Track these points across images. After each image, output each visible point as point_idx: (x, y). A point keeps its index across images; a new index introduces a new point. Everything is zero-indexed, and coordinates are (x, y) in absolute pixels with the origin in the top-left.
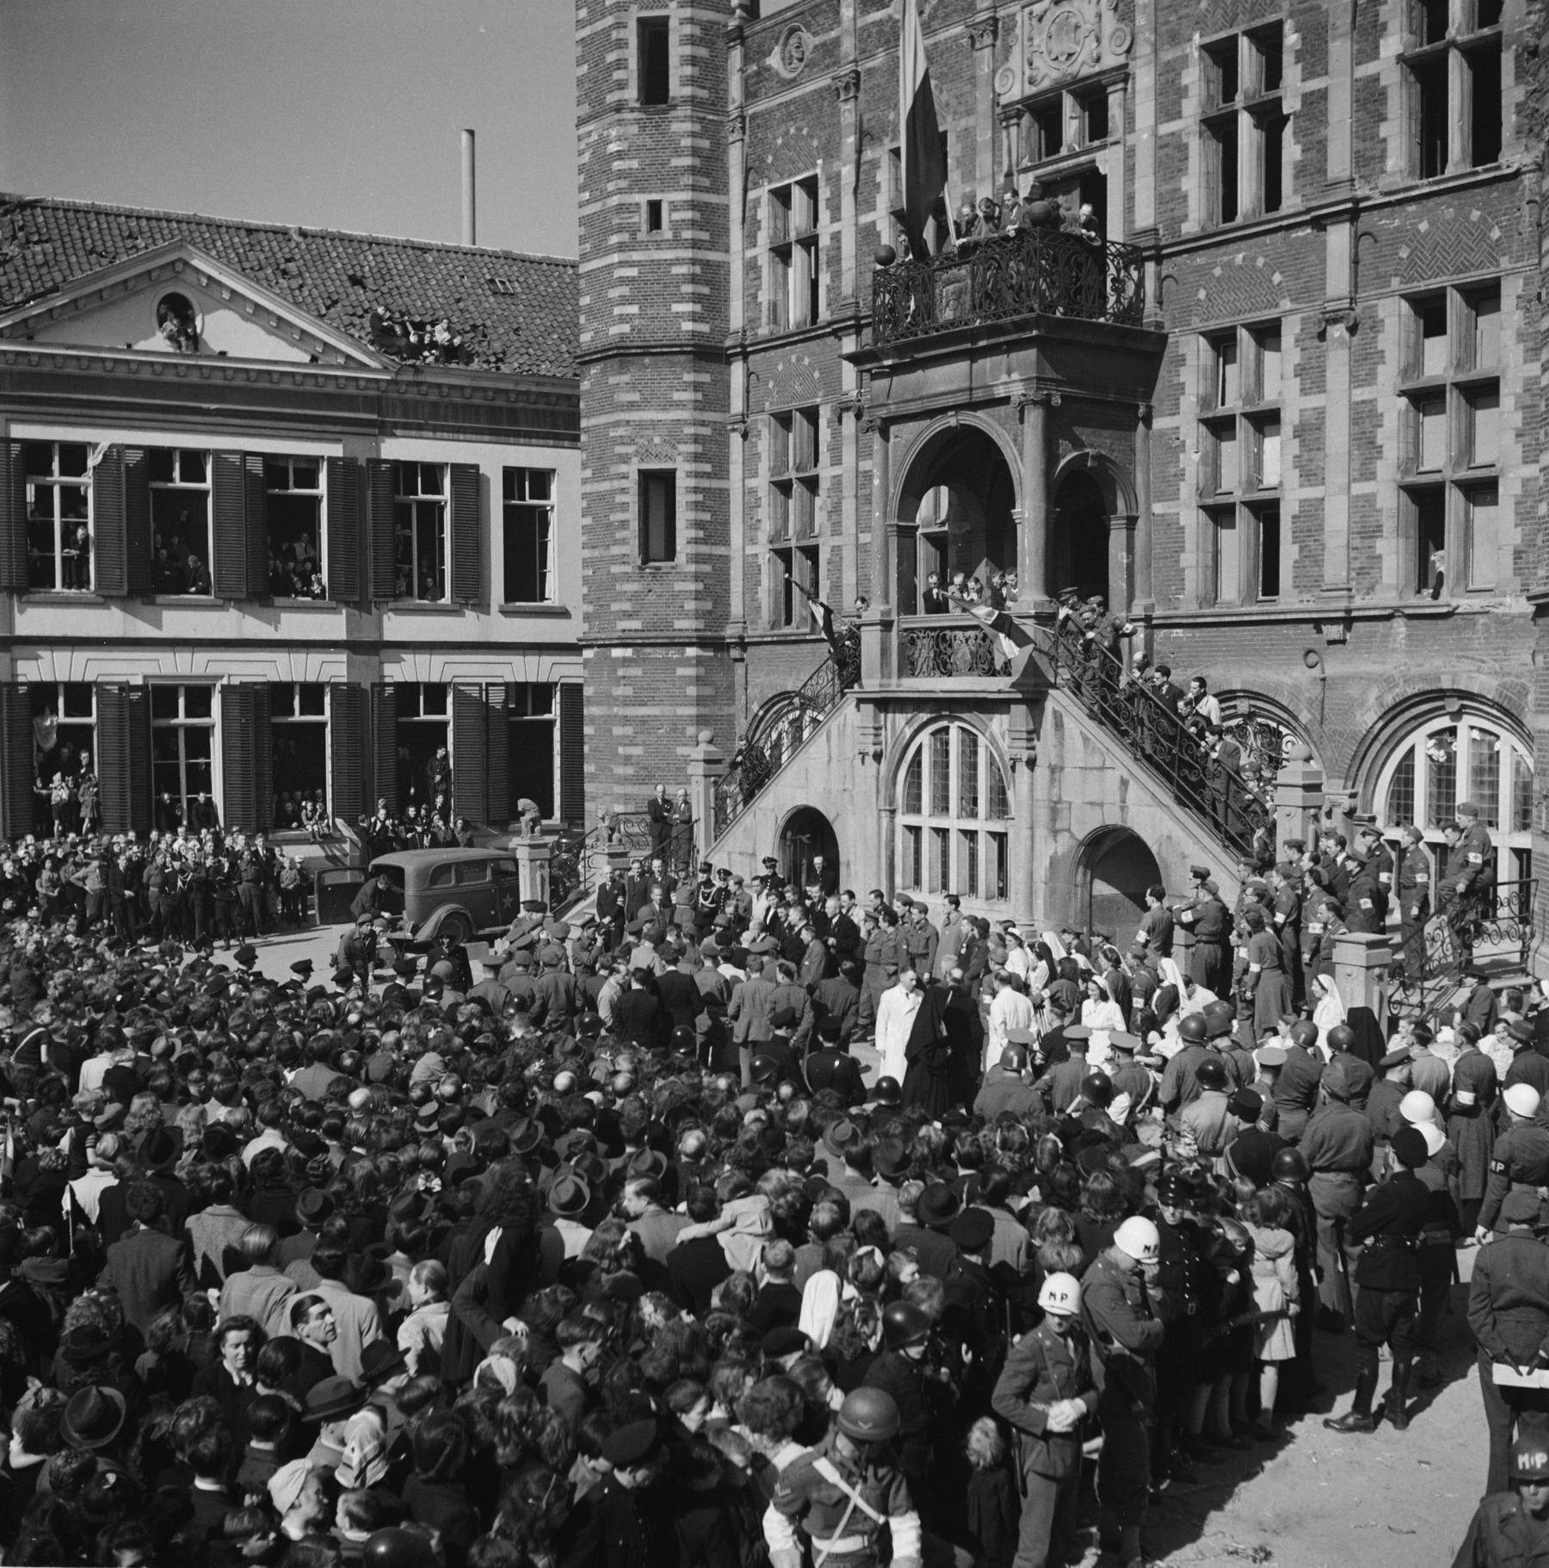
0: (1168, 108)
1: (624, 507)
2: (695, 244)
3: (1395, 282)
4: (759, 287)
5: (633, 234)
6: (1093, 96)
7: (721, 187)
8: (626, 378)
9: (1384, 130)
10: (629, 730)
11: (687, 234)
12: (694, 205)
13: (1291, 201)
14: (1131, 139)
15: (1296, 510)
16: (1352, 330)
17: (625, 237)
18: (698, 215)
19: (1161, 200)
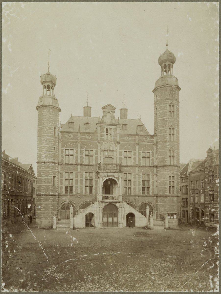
9: (141, 162)
17: (52, 150)
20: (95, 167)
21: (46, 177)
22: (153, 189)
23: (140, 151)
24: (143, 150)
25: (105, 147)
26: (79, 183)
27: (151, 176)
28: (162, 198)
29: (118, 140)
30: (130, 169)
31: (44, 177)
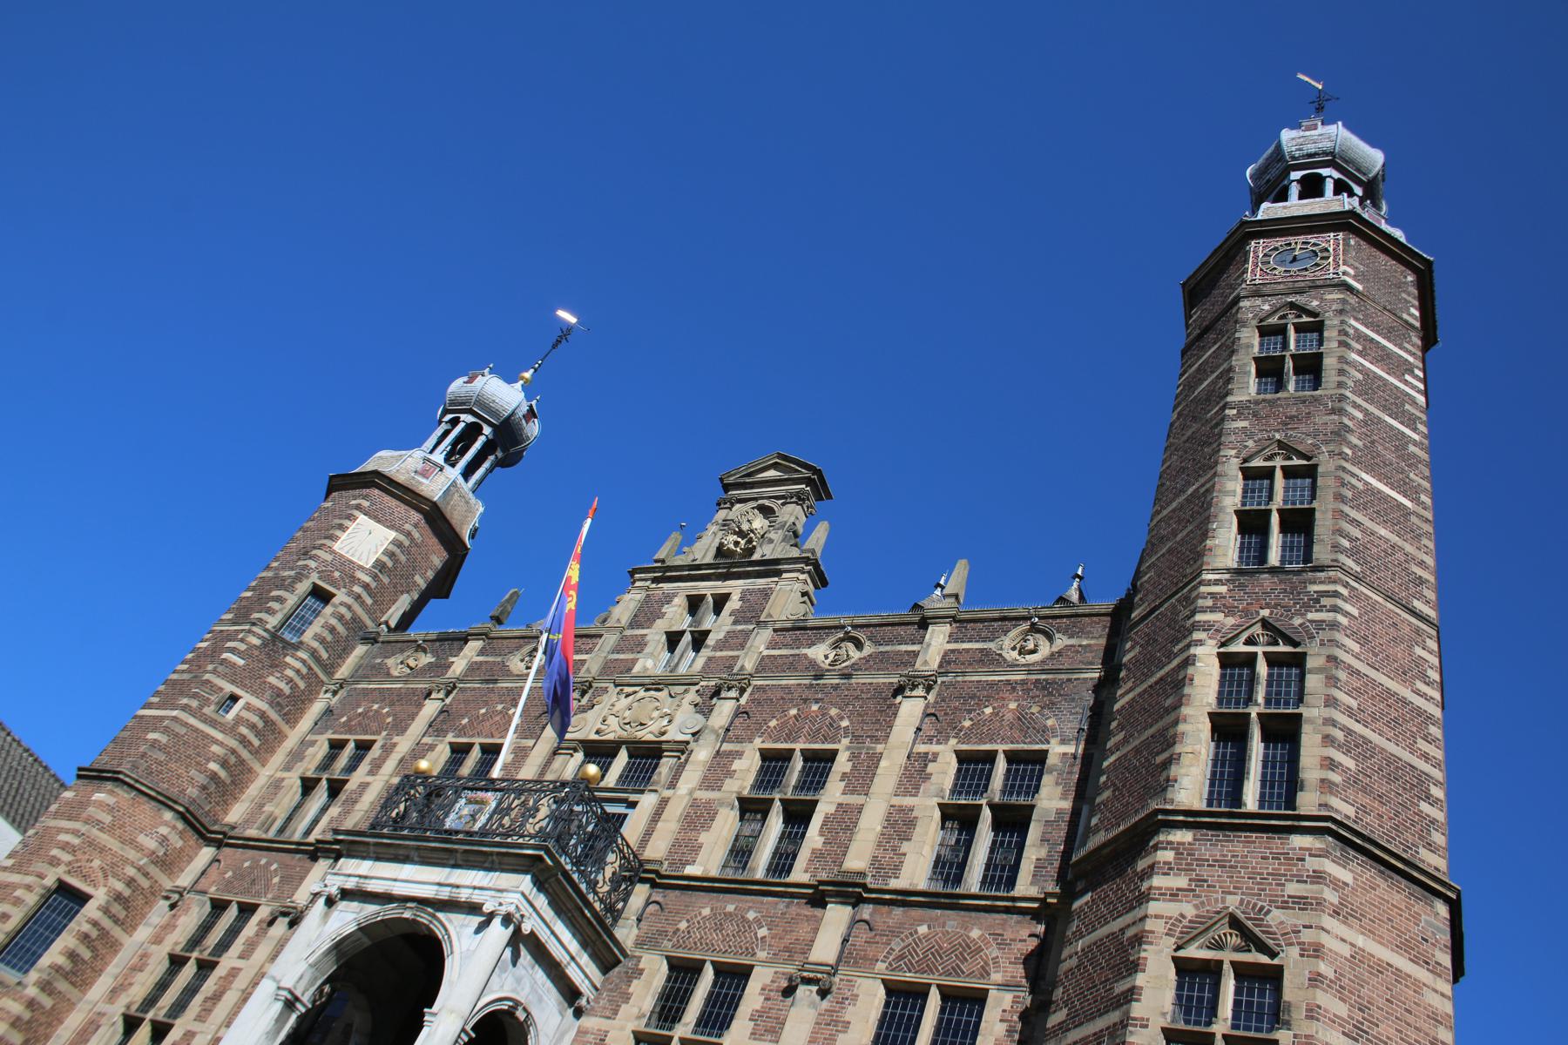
2: (244, 741)
3: (881, 966)
5: (201, 707)
6: (646, 755)
7: (292, 719)
8: (111, 800)
11: (244, 730)
12: (263, 715)
13: (799, 874)
14: (667, 793)
16: (823, 993)
17: (194, 703)
18: (260, 724)
19: (676, 844)
23: (934, 748)
25: (612, 721)
29: (748, 663)
30: (751, 915)
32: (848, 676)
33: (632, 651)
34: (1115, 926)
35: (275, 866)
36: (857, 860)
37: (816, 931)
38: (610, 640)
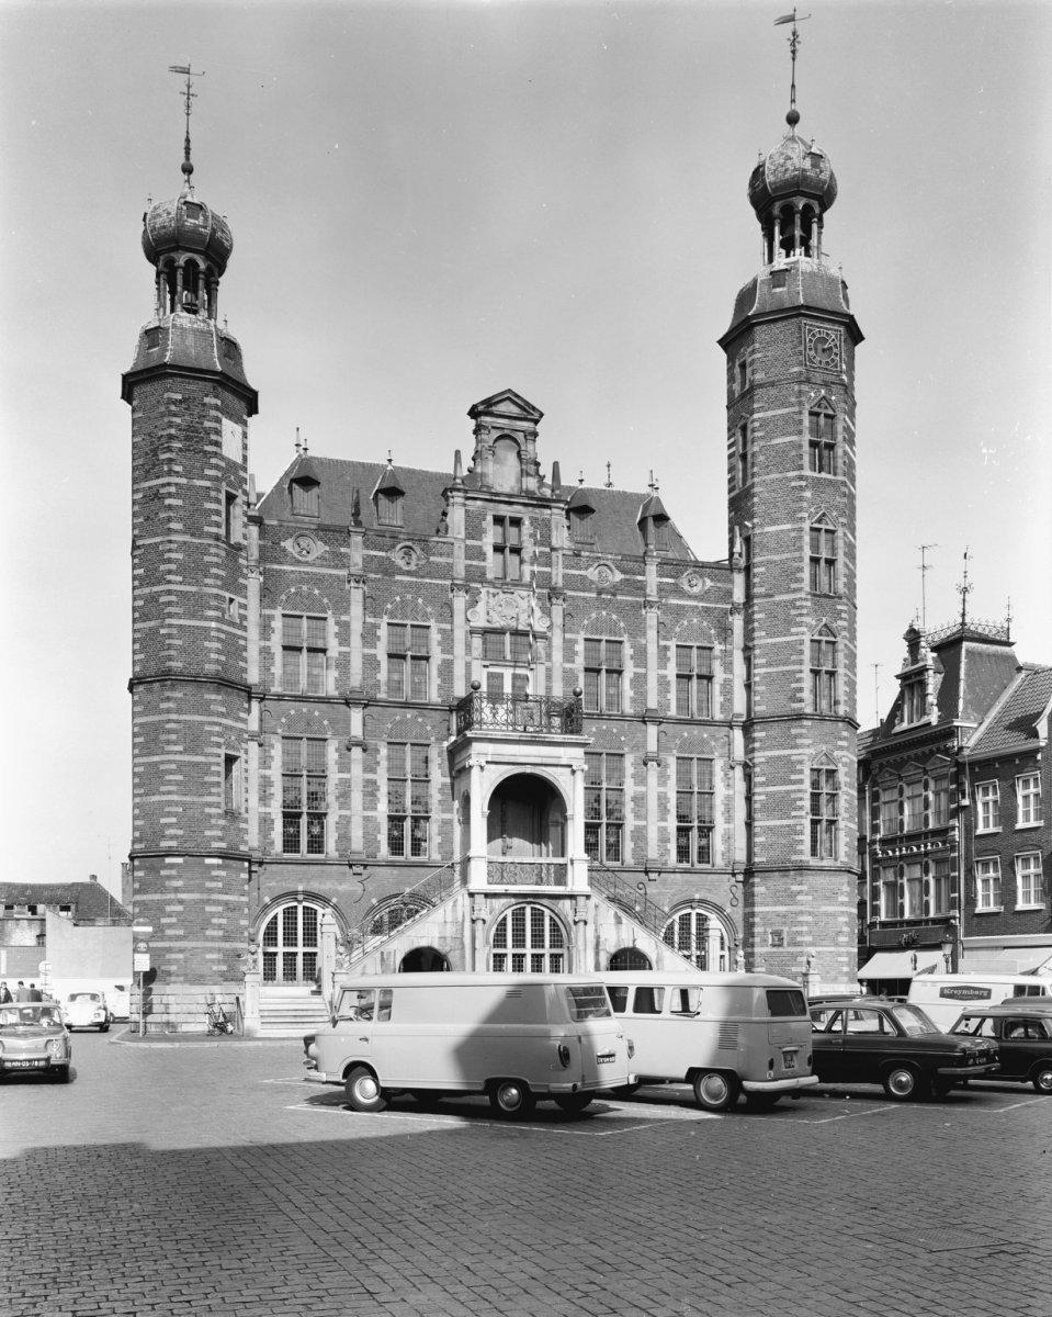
0: (569, 655)
1: (218, 774)
3: (675, 752)
4: (273, 664)
8: (220, 698)
10: (220, 909)
14: (548, 664)
15: (632, 829)
20: (437, 716)
21: (186, 758)
22: (728, 838)
24: (679, 638)
25: (491, 612)
26: (357, 798)
27: (718, 765)
28: (776, 881)
31: (178, 757)
32: (614, 595)
33: (478, 558)
34: (787, 752)
35: (317, 714)
36: (652, 703)
37: (645, 737)
38: (459, 552)
